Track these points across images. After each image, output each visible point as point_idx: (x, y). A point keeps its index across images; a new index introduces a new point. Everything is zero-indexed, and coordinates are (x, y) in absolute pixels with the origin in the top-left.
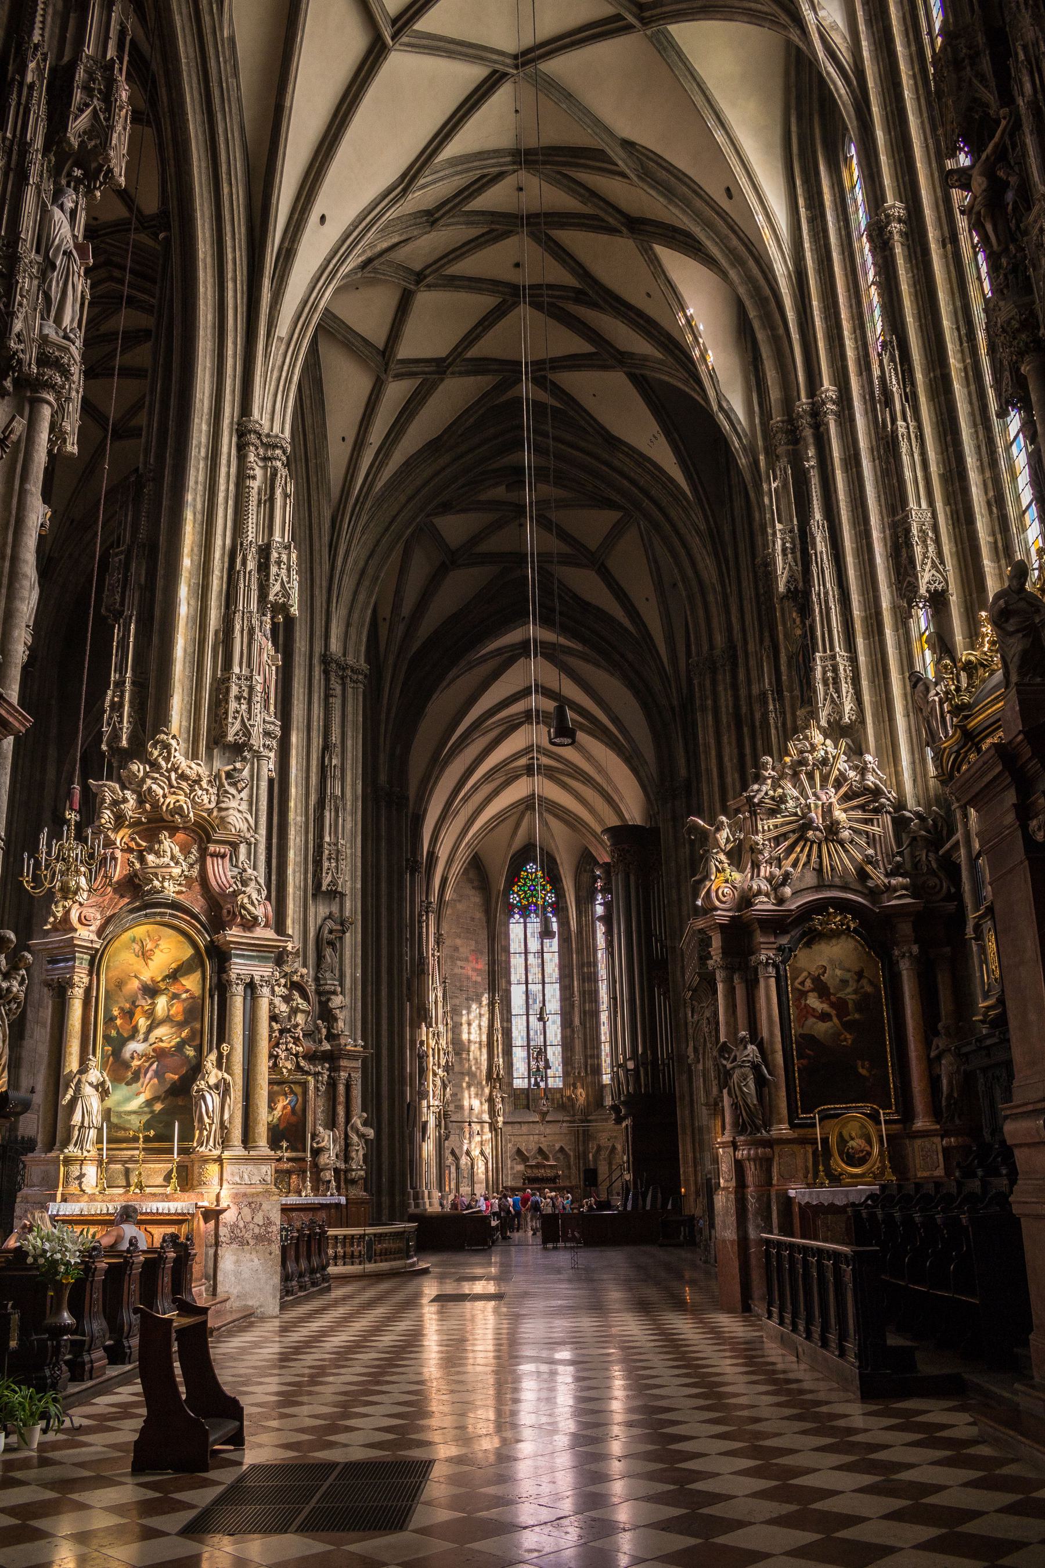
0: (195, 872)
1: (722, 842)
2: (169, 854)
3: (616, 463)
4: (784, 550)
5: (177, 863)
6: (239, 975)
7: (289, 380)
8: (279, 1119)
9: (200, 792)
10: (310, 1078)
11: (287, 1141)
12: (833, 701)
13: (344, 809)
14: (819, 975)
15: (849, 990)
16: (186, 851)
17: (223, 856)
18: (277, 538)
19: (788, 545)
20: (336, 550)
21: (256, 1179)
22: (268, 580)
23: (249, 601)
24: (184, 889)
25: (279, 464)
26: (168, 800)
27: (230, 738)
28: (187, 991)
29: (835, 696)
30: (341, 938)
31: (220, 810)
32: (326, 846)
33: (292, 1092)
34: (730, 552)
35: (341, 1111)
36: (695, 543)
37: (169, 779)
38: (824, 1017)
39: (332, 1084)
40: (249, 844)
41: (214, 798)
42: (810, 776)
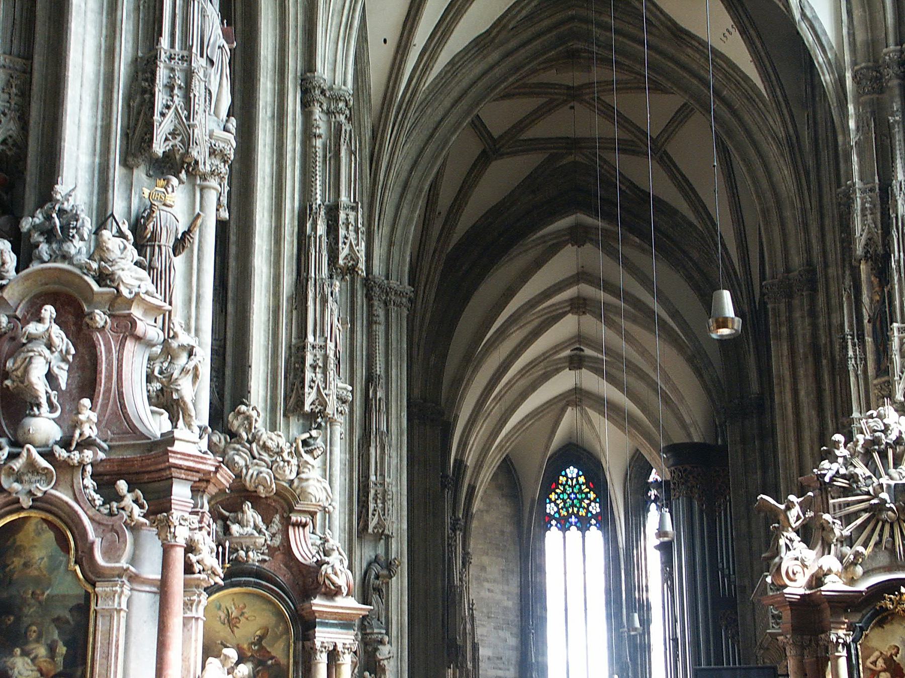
0: (277, 542)
1: (792, 520)
2: (252, 524)
3: (683, 58)
4: (863, 209)
5: (260, 532)
6: (323, 643)
9: (282, 464)
13: (390, 446)
16: (268, 522)
18: (344, 198)
19: (867, 205)
20: (377, 164)
22: (337, 243)
23: (319, 266)
24: (267, 558)
25: (342, 118)
26: (250, 472)
27: (307, 408)
28: (272, 658)
30: (387, 583)
31: (301, 480)
32: (372, 485)
34: (811, 163)
36: (772, 150)
41: (295, 469)
42: (883, 455)
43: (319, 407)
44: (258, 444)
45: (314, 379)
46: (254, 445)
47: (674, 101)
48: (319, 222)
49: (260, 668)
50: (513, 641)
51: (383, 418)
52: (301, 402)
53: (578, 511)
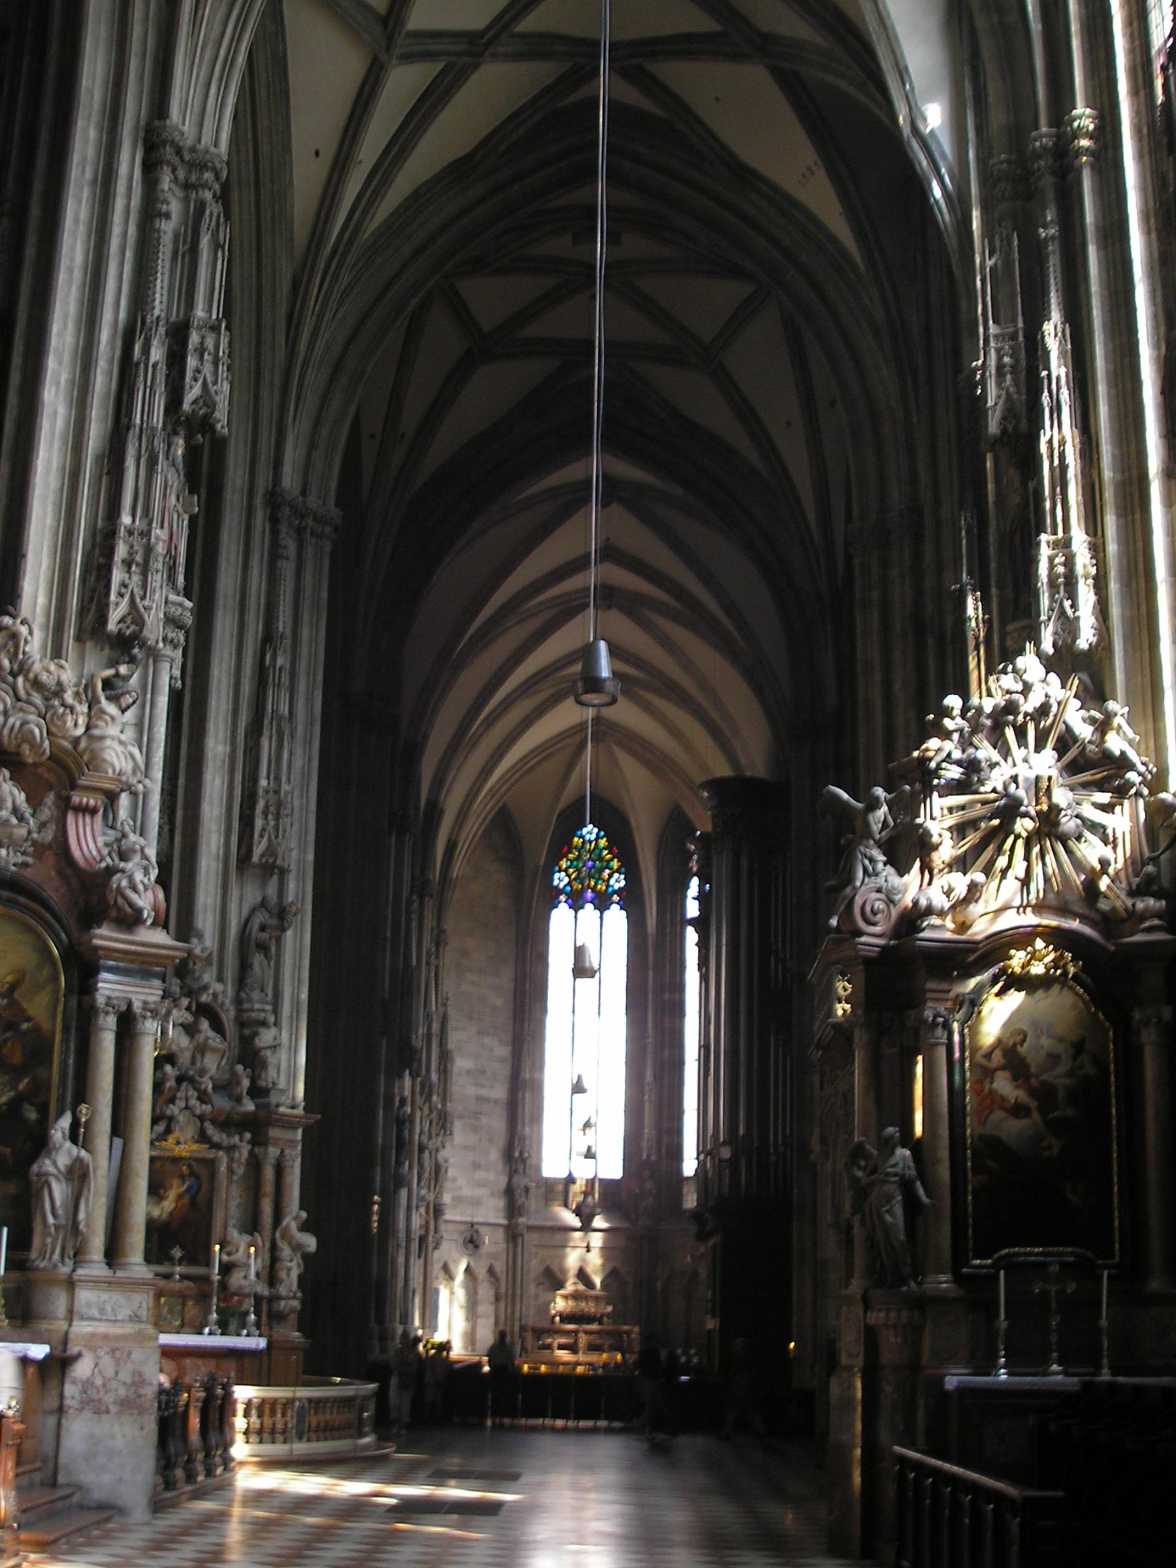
0: (49, 835)
1: (876, 828)
2: (9, 804)
4: (1000, 367)
5: (21, 819)
6: (109, 998)
7: (229, 62)
8: (171, 1214)
9: (61, 710)
10: (221, 1153)
11: (183, 1248)
12: (1062, 613)
13: (292, 737)
14: (1014, 1045)
15: (1062, 1069)
16: (34, 801)
17: (93, 812)
18: (200, 312)
20: (298, 325)
21: (123, 1314)
24: (30, 860)
25: (208, 195)
26: (11, 720)
27: (112, 626)
28: (29, 1019)
29: (1067, 604)
30: (279, 940)
32: (261, 792)
33: (192, 1173)
35: (267, 1206)
37: (14, 688)
38: (1018, 1110)
39: (255, 1165)
40: (134, 794)
41: (82, 720)
42: (1021, 733)
43: (133, 627)
44: (26, 679)
45: (127, 581)
46: (20, 680)
47: (732, 292)
48: (155, 342)
49: (8, 1034)
50: (504, 1051)
51: (284, 697)
52: (103, 619)
53: (596, 884)
